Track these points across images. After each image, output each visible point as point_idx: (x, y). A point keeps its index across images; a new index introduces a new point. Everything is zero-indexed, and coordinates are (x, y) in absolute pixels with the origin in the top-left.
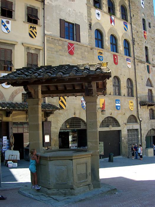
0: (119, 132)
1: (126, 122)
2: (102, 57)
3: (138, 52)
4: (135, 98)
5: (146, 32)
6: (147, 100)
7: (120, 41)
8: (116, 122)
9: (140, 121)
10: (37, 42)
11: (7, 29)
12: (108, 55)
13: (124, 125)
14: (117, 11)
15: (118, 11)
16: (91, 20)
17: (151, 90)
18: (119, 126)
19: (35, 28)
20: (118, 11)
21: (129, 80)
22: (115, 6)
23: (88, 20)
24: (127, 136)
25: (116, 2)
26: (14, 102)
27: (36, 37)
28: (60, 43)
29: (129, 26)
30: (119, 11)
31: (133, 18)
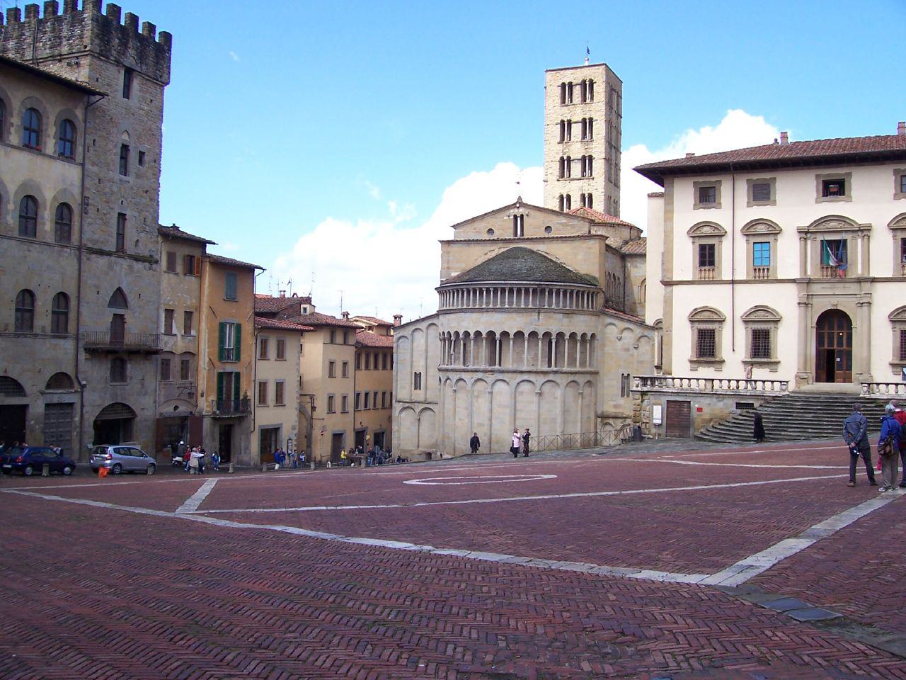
1: (42, 387)
3: (96, 230)
6: (108, 338)
7: (46, 210)
9: (83, 387)
13: (38, 394)
14: (48, 139)
15: (49, 137)
17: (122, 316)
18: (25, 395)
20: (52, 137)
21: (62, 297)
22: (44, 127)
30: (54, 138)
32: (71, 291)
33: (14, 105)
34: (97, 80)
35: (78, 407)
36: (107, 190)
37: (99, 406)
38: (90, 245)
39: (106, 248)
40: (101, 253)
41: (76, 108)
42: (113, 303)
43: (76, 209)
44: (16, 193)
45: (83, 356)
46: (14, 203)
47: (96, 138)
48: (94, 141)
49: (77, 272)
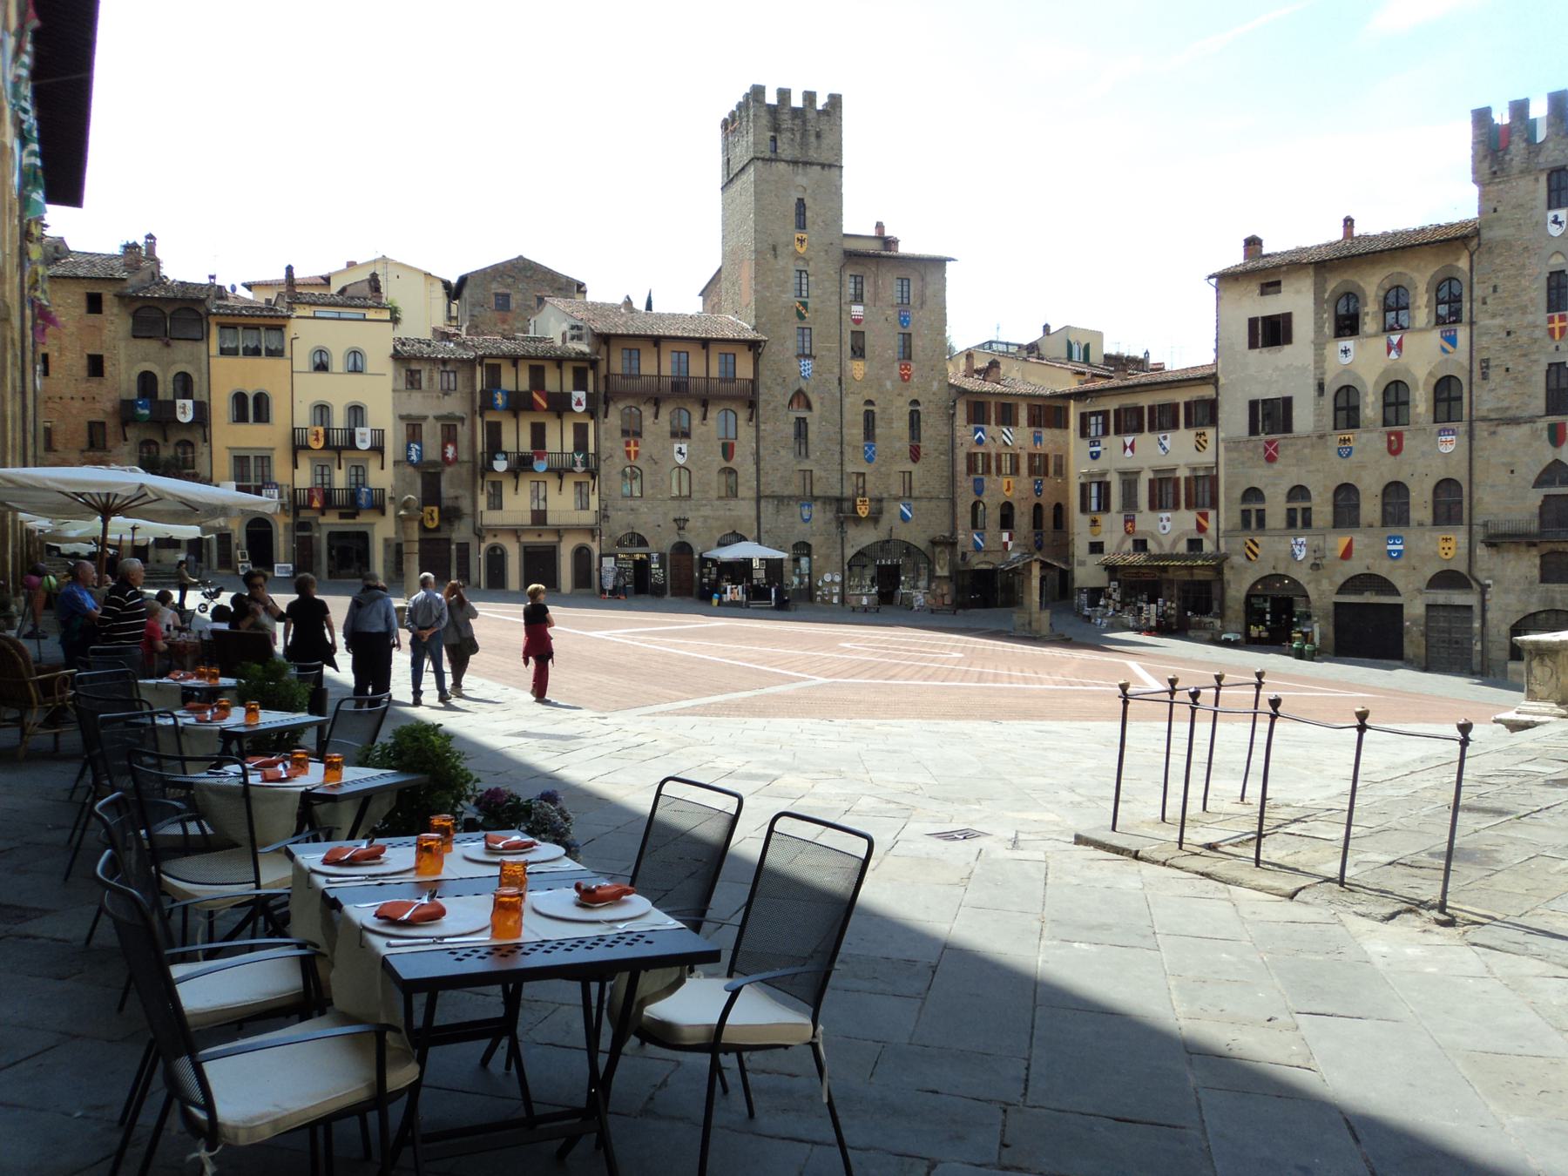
0: (1400, 607)
1: (1423, 585)
2: (1351, 448)
4: (1464, 529)
5: (1556, 315)
6: (1534, 527)
7: (1417, 388)
8: (1388, 588)
10: (1207, 457)
11: (1164, 449)
12: (1369, 440)
16: (1323, 374)
18: (1399, 595)
19: (1204, 434)
23: (1315, 375)
24: (1423, 621)
25: (1418, 284)
26: (1175, 553)
27: (1204, 448)
28: (1251, 445)
29: (1462, 333)
31: (1489, 301)
32: (1460, 475)
33: (1367, 293)
34: (1495, 210)
35: (1477, 610)
36: (1524, 339)
37: (1517, 612)
38: (1493, 416)
39: (1525, 414)
40: (1515, 421)
41: (1458, 260)
42: (1539, 483)
43: (1465, 382)
44: (1377, 383)
45: (1481, 551)
46: (1374, 394)
47: (1494, 281)
48: (1495, 289)
49: (1467, 453)
